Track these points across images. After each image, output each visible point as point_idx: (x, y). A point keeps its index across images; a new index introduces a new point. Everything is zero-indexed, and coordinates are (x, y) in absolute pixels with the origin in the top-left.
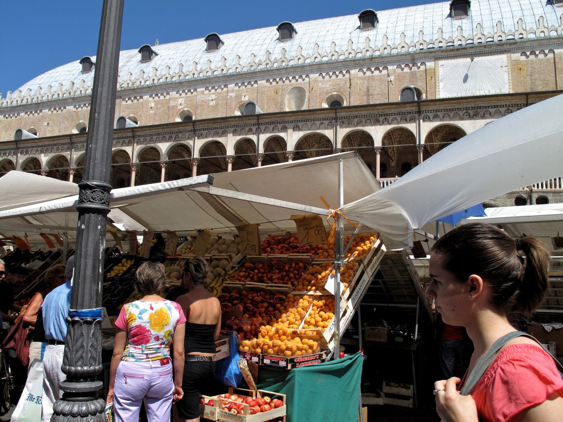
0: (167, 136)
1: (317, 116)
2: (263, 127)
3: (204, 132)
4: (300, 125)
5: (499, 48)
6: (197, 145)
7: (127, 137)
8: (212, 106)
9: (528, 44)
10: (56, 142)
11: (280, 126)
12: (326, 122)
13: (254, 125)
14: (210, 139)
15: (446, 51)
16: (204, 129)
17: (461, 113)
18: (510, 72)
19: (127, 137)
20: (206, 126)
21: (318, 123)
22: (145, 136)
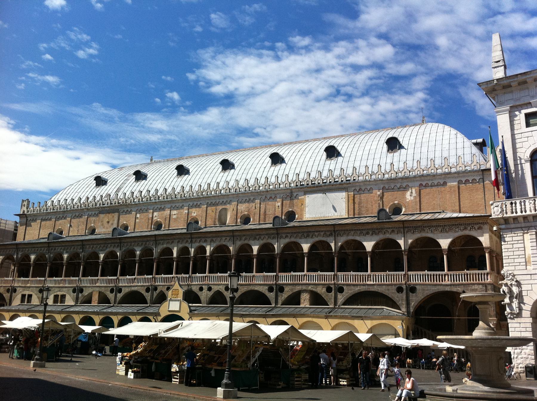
0: (140, 243)
1: (223, 234)
2: (194, 240)
3: (162, 242)
4: (214, 239)
5: (341, 186)
6: (156, 251)
7: (117, 243)
8: (175, 219)
9: (357, 184)
10: (73, 244)
11: (203, 240)
12: (228, 238)
13: (189, 238)
14: (165, 246)
15: (310, 187)
16: (162, 240)
17: (300, 235)
18: (347, 202)
19: (117, 243)
20: (162, 238)
21: (224, 238)
22: (127, 242)
